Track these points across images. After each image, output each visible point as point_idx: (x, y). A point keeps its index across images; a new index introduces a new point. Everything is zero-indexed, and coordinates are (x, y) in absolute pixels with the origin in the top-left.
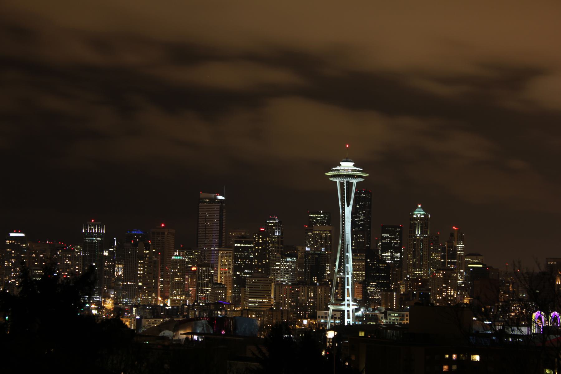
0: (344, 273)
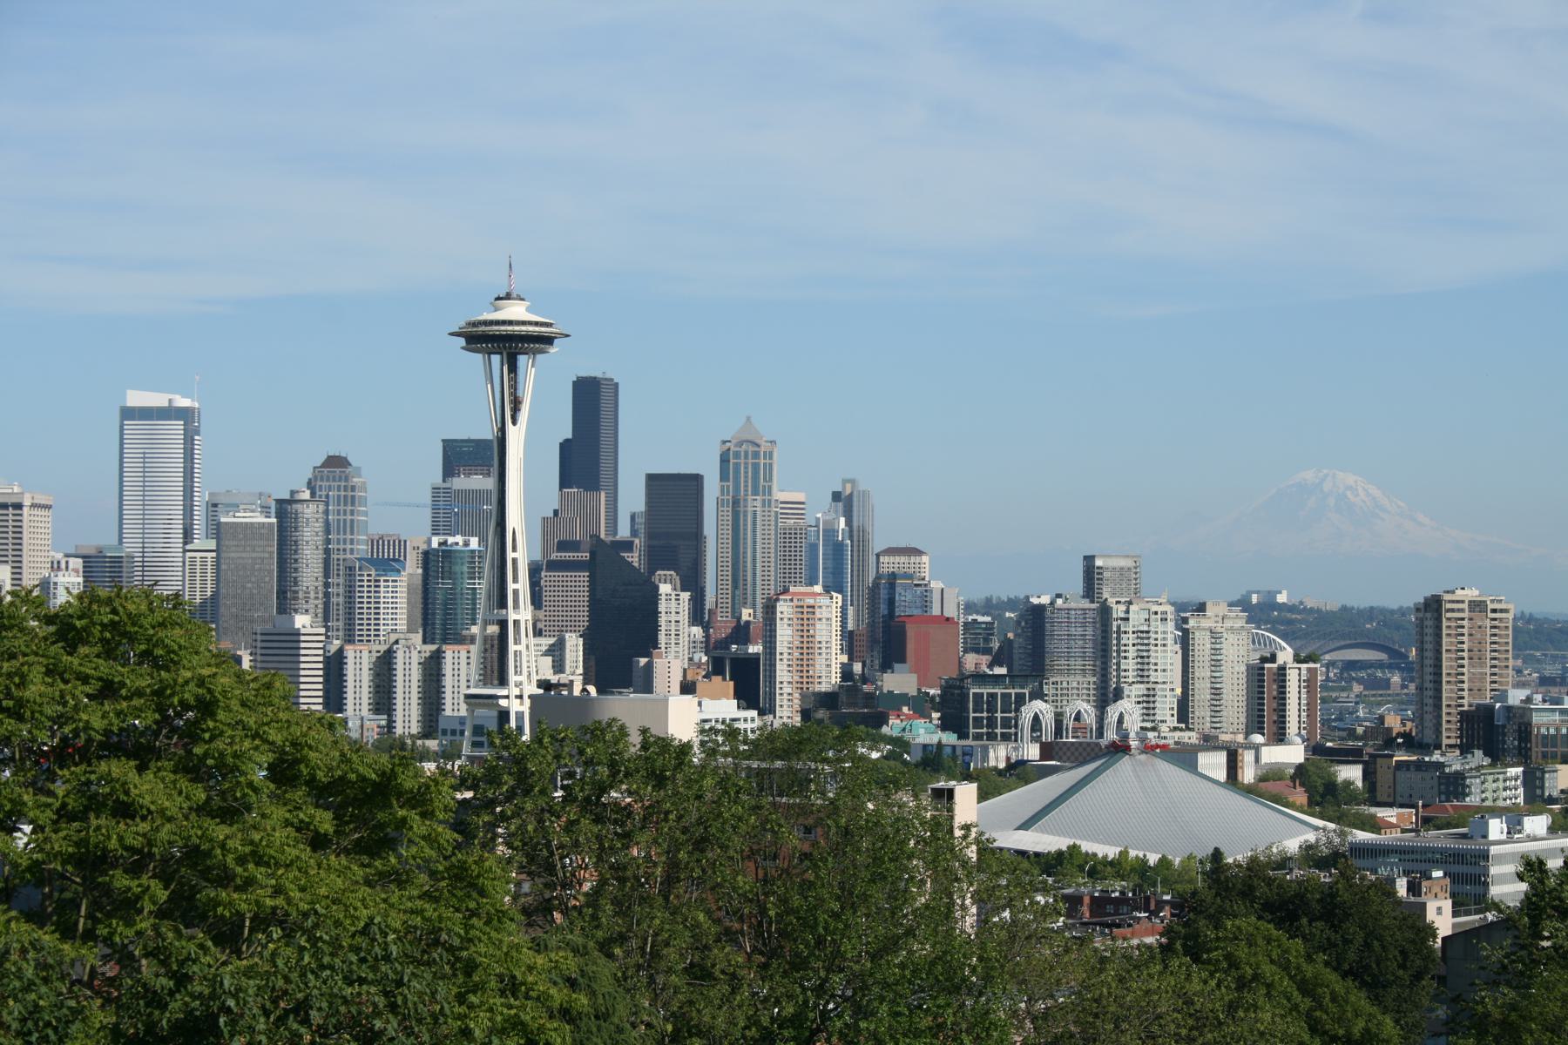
0: (503, 604)
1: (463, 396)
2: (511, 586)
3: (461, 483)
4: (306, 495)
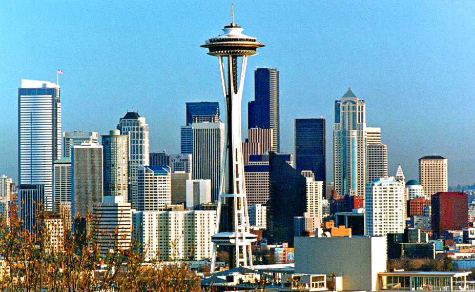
0: (231, 191)
1: (208, 79)
2: (235, 179)
3: (195, 126)
4: (118, 132)
